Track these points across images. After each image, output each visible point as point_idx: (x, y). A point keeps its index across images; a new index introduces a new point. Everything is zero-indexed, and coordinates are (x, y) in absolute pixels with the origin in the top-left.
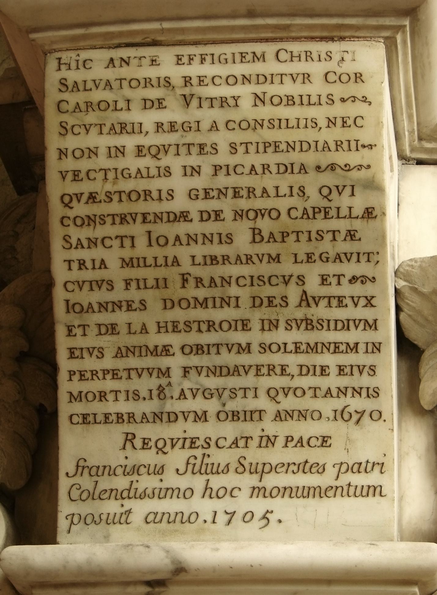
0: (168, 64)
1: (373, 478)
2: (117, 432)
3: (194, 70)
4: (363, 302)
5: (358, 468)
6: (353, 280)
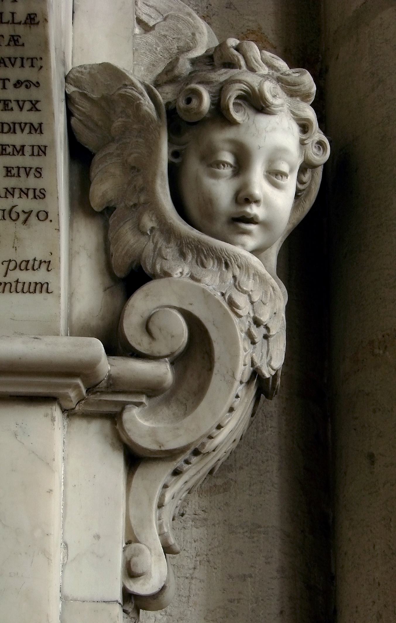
1: (40, 276)
4: (27, 106)
5: (26, 265)
6: (18, 84)
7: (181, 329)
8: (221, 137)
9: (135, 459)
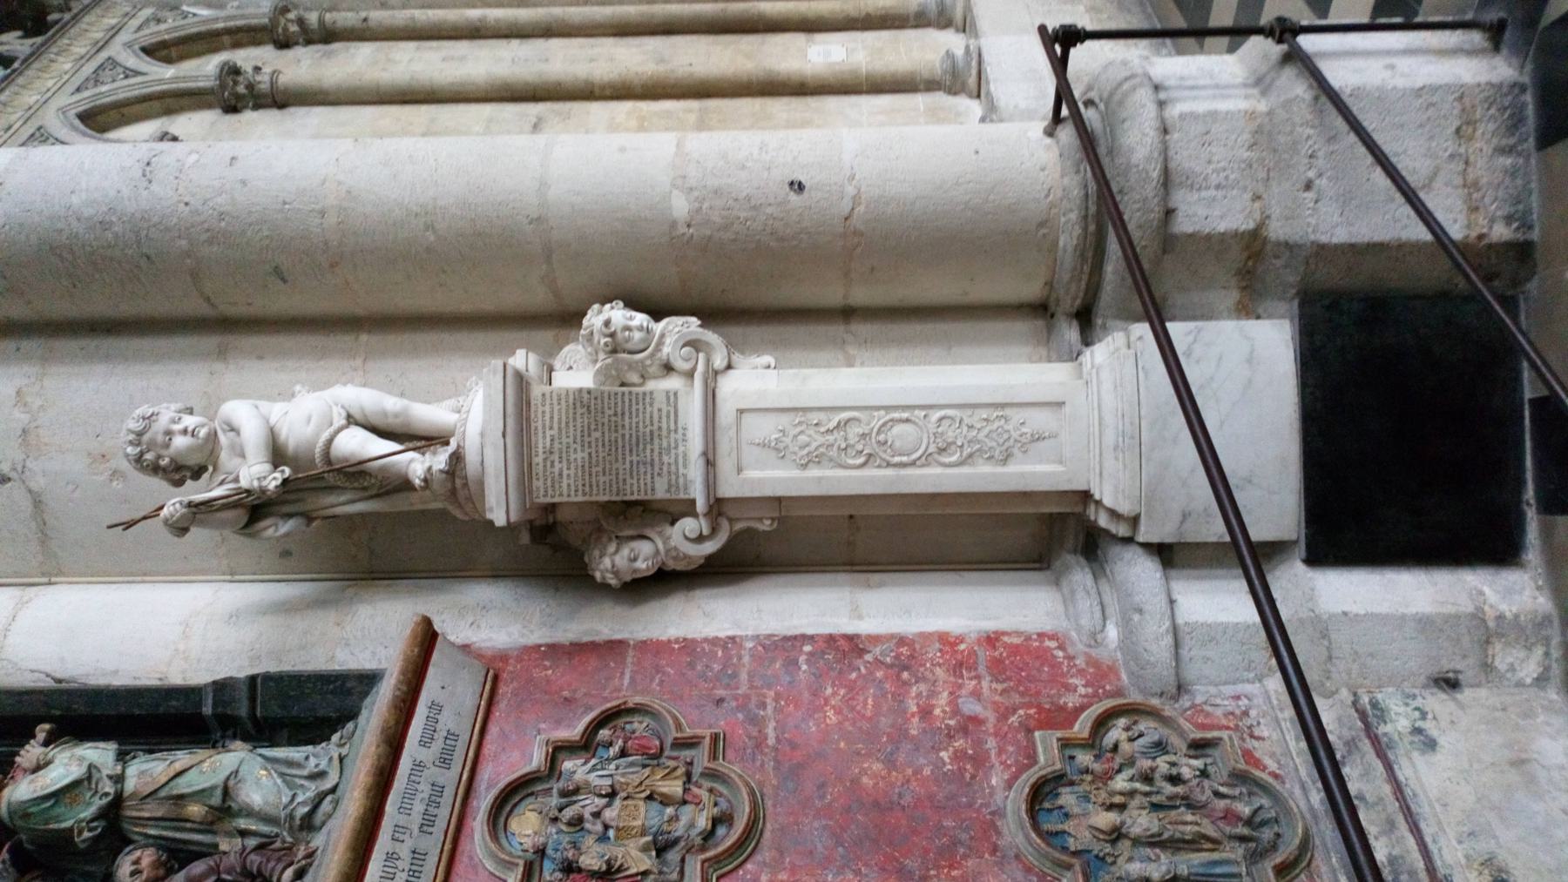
0: (539, 459)
2: (657, 478)
3: (541, 450)
5: (668, 398)
7: (687, 349)
8: (619, 335)
9: (729, 367)
